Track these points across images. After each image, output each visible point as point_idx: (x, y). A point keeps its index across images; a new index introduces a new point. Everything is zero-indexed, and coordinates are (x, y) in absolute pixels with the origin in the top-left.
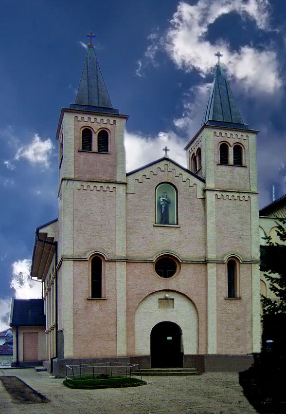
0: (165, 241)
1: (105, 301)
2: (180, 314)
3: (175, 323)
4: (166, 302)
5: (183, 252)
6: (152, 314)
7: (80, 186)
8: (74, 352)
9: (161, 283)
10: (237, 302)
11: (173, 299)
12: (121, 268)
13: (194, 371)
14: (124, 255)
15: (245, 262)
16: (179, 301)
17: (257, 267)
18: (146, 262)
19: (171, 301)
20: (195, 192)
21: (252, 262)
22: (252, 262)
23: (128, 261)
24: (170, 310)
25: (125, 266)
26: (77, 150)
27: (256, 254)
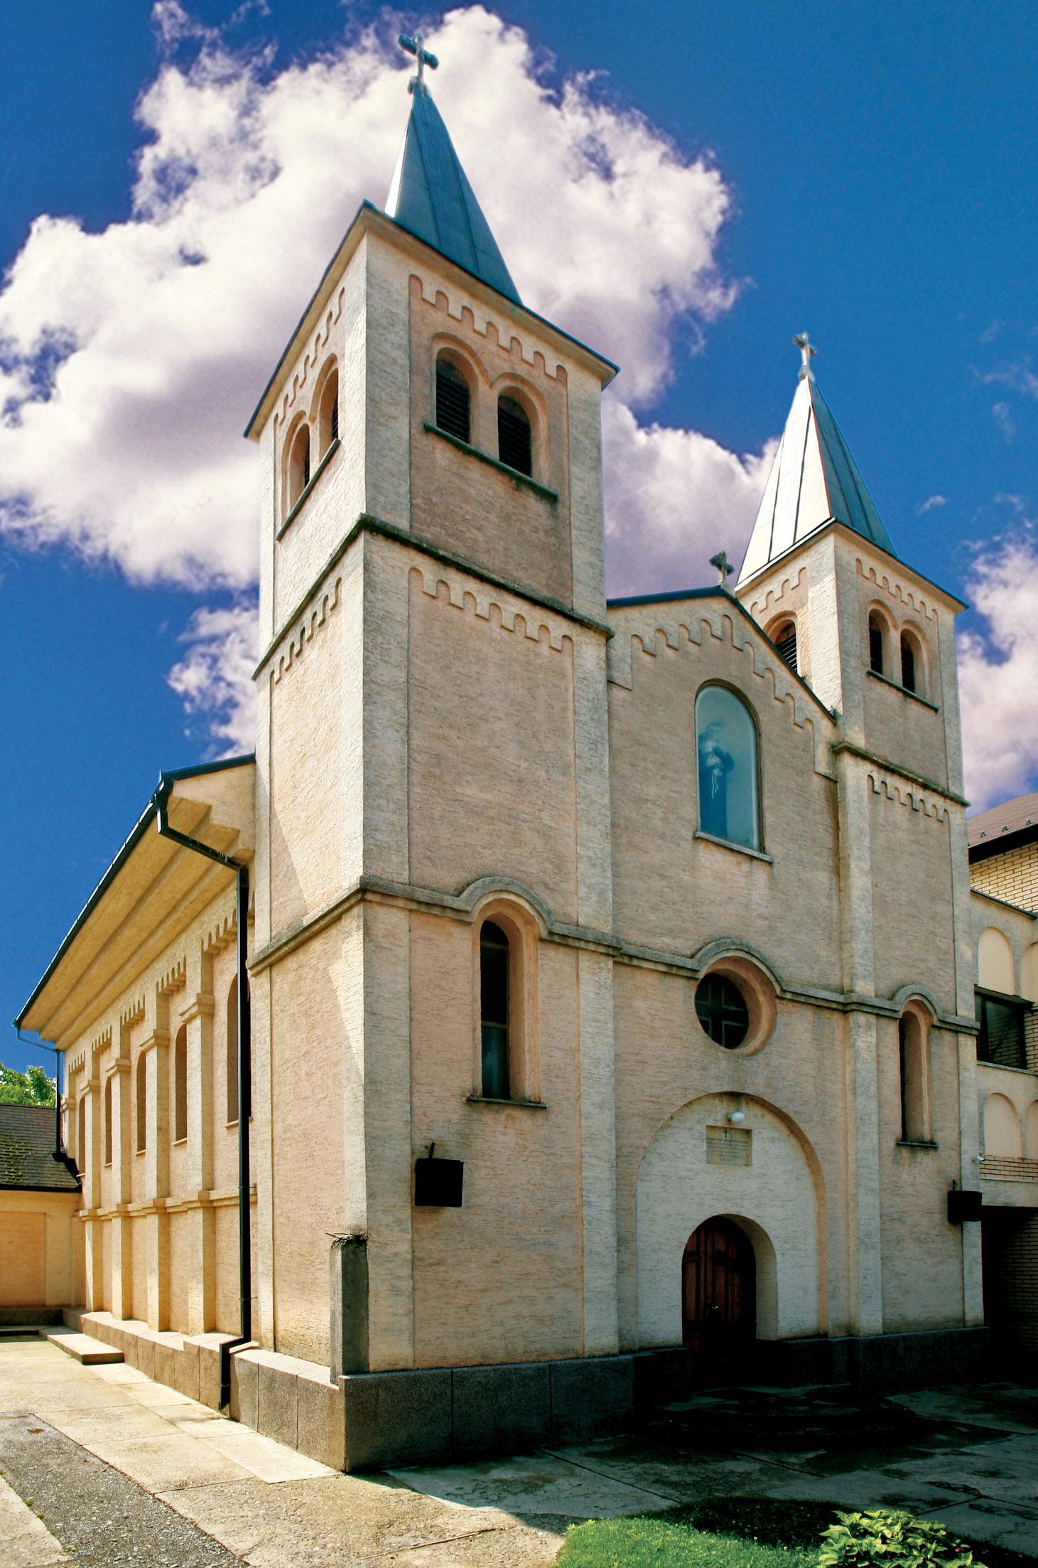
0: (723, 898)
1: (540, 1116)
2: (764, 1185)
3: (753, 1222)
4: (730, 1142)
5: (796, 957)
6: (692, 1184)
7: (486, 607)
8: (414, 1340)
9: (719, 1068)
10: (524, 1119)
11: (748, 1133)
12: (593, 980)
13: (732, 1407)
14: (605, 927)
15: (803, 1000)
16: (769, 1141)
17: (969, 1046)
18: (672, 970)
19: (739, 1137)
20: (807, 747)
21: (957, 1030)
22: (957, 1030)
23: (620, 955)
24: (741, 1172)
25: (610, 976)
26: (417, 421)
27: (967, 1011)
